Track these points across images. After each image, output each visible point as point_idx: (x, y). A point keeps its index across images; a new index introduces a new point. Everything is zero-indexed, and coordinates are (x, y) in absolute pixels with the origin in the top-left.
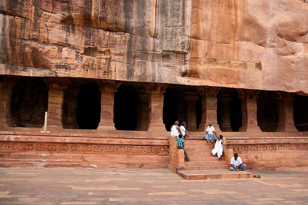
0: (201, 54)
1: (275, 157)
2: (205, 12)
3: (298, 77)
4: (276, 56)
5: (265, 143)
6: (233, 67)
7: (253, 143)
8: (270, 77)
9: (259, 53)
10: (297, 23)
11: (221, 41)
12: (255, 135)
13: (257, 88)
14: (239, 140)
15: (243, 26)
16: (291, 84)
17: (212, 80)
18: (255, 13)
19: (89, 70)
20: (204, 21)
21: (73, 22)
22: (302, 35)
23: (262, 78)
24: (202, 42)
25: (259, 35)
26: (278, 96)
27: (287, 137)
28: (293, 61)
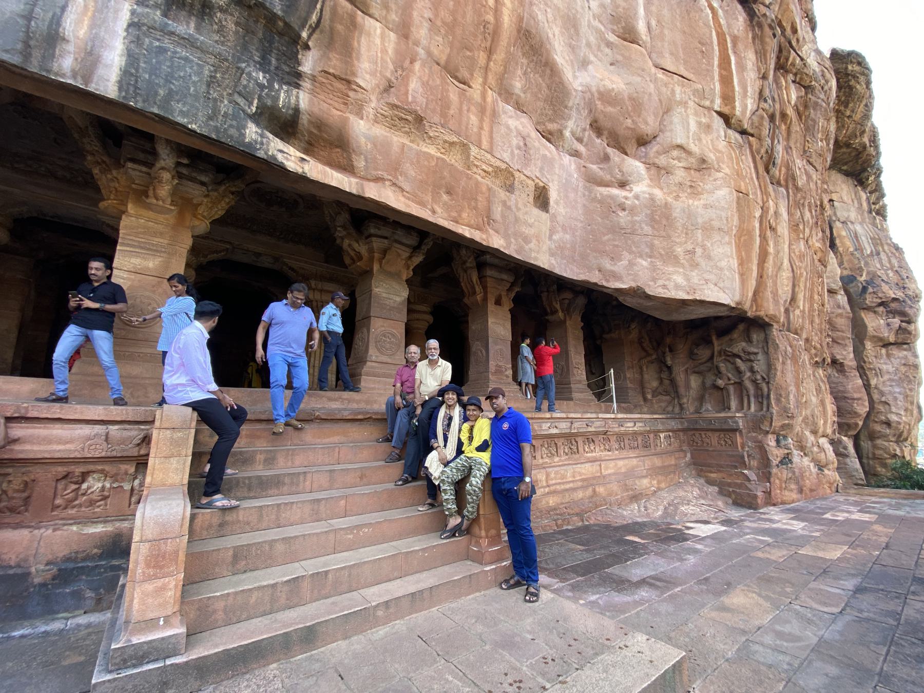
3: (634, 249)
5: (554, 431)
6: (475, 170)
8: (568, 237)
9: (544, 156)
17: (403, 190)
22: (643, 142)
24: (376, 29)
26: (557, 311)
27: (601, 416)
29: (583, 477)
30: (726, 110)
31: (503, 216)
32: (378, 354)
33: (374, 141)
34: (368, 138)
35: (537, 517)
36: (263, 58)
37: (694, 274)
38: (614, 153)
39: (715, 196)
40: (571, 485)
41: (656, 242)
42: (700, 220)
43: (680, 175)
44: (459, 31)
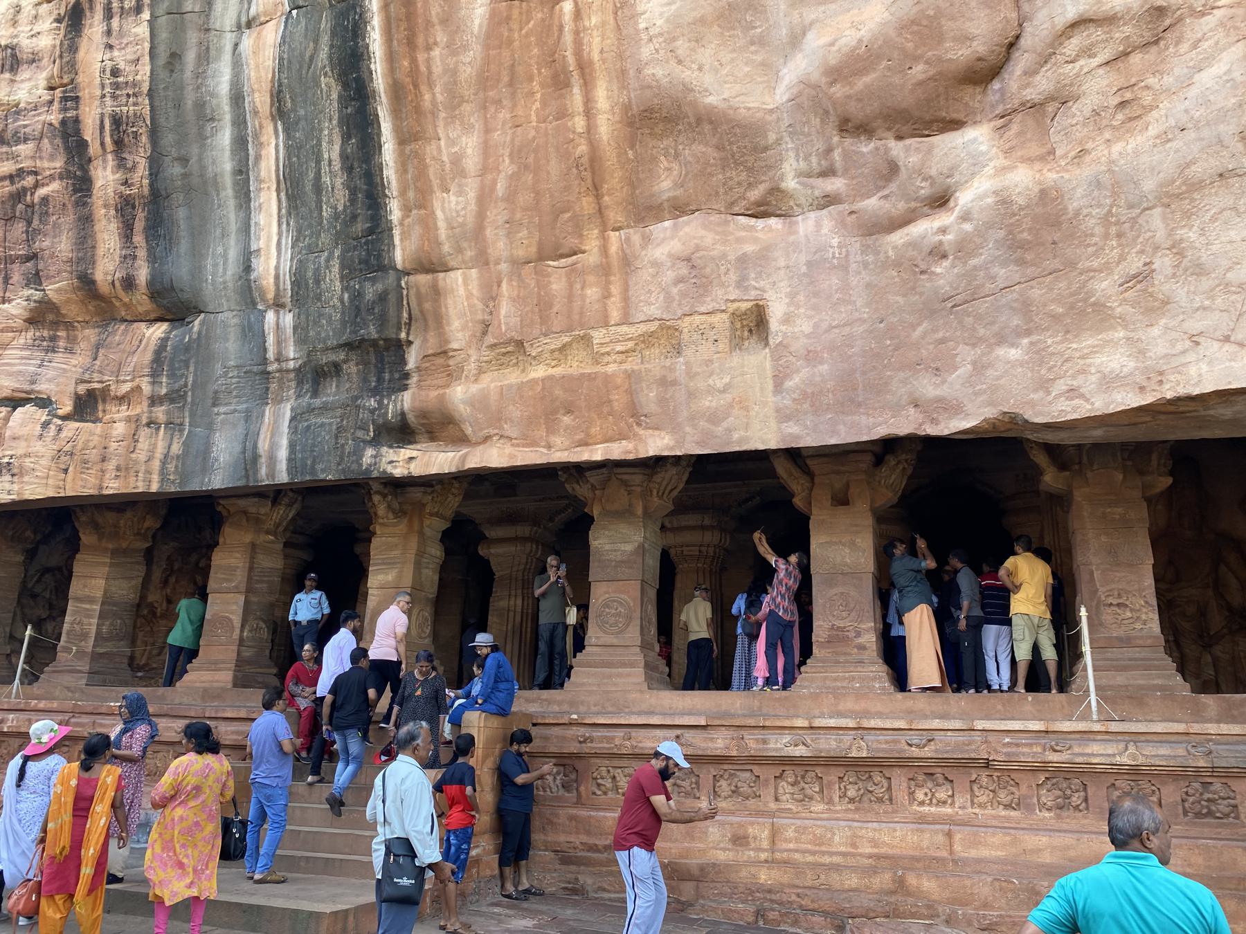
0: (458, 332)
1: (869, 850)
4: (855, 244)
6: (607, 359)
7: (718, 753)
9: (743, 260)
10: (929, 16)
11: (534, 249)
14: (643, 732)
15: (632, 147)
16: (944, 382)
17: (511, 439)
18: (680, 62)
19: (71, 469)
21: (64, 316)
22: (984, 73)
23: (770, 385)
25: (734, 165)
28: (941, 243)
31: (662, 401)
32: (601, 634)
33: (471, 403)
34: (464, 402)
35: (721, 894)
36: (380, 380)
37: (1155, 331)
38: (907, 149)
39: (1193, 92)
41: (1036, 293)
42: (1149, 185)
44: (546, 202)
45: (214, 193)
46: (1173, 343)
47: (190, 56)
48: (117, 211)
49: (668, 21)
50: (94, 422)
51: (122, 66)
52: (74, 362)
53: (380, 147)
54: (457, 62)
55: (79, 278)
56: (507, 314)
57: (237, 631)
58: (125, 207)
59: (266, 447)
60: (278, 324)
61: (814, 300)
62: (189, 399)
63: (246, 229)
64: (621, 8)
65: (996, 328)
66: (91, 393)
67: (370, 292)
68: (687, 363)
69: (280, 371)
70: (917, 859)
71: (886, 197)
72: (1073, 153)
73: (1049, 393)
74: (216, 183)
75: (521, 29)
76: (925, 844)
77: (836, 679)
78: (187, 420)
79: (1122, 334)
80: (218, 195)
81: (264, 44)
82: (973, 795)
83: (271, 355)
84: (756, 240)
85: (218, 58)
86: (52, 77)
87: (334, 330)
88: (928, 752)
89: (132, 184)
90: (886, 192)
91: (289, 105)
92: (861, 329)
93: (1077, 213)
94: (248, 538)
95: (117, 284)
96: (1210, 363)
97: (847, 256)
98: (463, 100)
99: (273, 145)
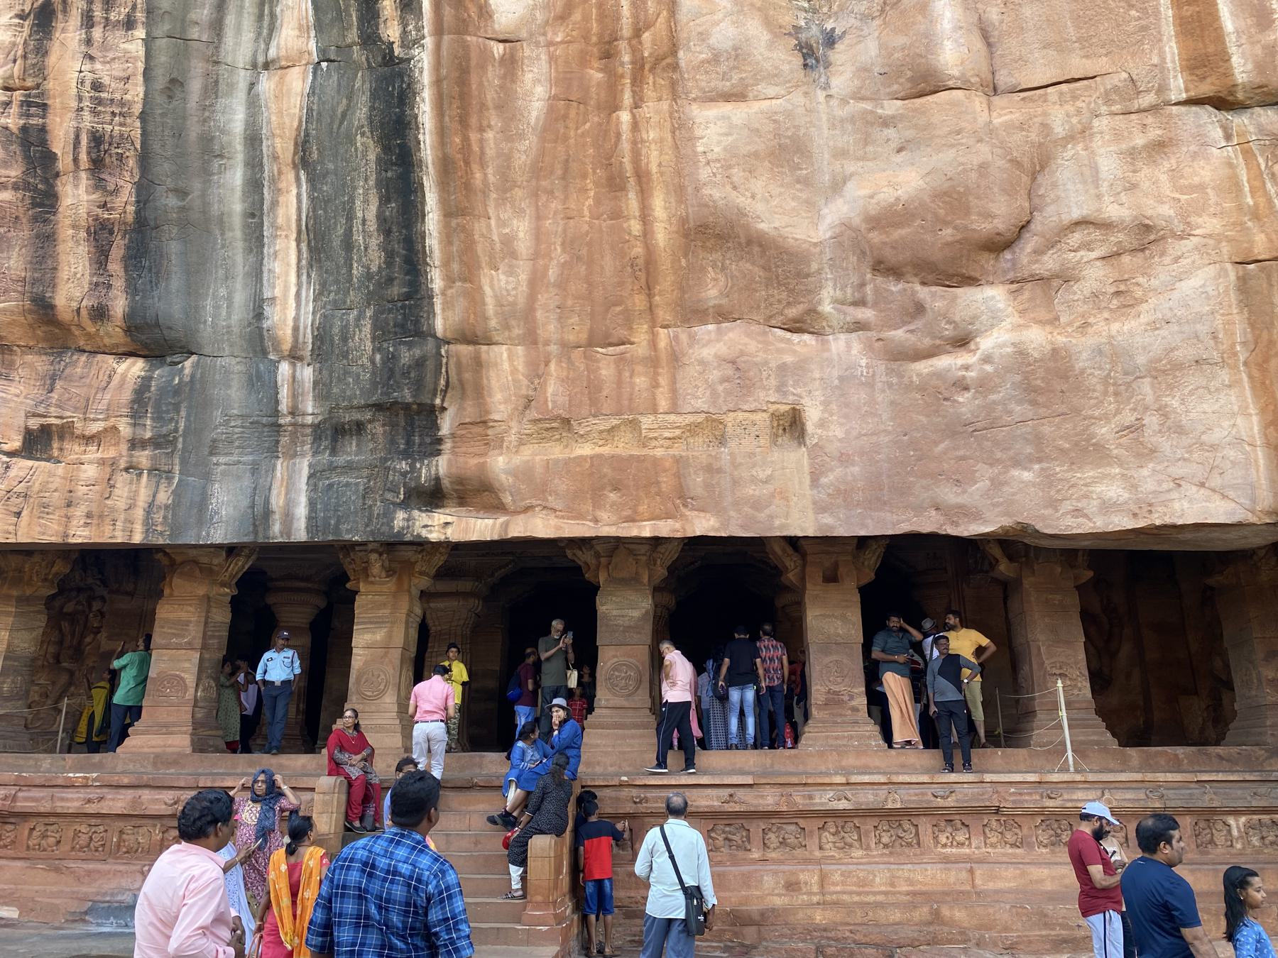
0: (500, 404)
2: (502, 223)
3: (999, 455)
4: (881, 367)
5: (843, 805)
6: (654, 443)
7: (770, 808)
9: (783, 368)
10: (959, 193)
11: (584, 336)
12: (844, 763)
13: (782, 526)
15: (686, 256)
16: (964, 492)
17: (555, 511)
18: (735, 188)
20: (501, 267)
22: (999, 245)
23: (807, 481)
25: (775, 282)
26: (994, 564)
27: (988, 777)
29: (918, 888)
30: (1206, 89)
31: (708, 486)
32: (610, 696)
33: (514, 473)
34: (507, 472)
35: (782, 936)
36: (409, 443)
37: (1145, 472)
38: (934, 295)
39: (1176, 295)
40: (880, 898)
41: (1047, 429)
42: (1141, 360)
43: (1095, 276)
45: (217, 232)
46: (1160, 483)
47: (195, 86)
48: (89, 233)
49: (725, 149)
50: (45, 460)
51: (106, 80)
52: (13, 390)
53: (424, 216)
54: (511, 149)
55: (33, 300)
56: (554, 391)
57: (192, 691)
58: (100, 233)
59: (281, 502)
60: (294, 377)
61: (845, 410)
62: (180, 446)
63: (257, 274)
64: (679, 129)
65: (1011, 453)
66: (46, 431)
67: (406, 357)
68: (731, 454)
69: (292, 425)
70: (946, 894)
71: (912, 331)
72: (1078, 324)
73: (1057, 511)
74: (221, 221)
75: (577, 129)
76: (952, 880)
77: (837, 738)
78: (177, 468)
79: (1117, 471)
80: (222, 234)
81: (289, 91)
82: (986, 837)
83: (284, 406)
84: (794, 352)
85: (229, 94)
86: (11, 77)
87: (361, 389)
88: (950, 802)
89: (112, 209)
90: (912, 327)
91: (315, 156)
92: (887, 439)
93: (1083, 371)
94: (201, 590)
95: (84, 313)
96: (1190, 501)
97: (873, 375)
98: (515, 185)
99: (294, 191)
